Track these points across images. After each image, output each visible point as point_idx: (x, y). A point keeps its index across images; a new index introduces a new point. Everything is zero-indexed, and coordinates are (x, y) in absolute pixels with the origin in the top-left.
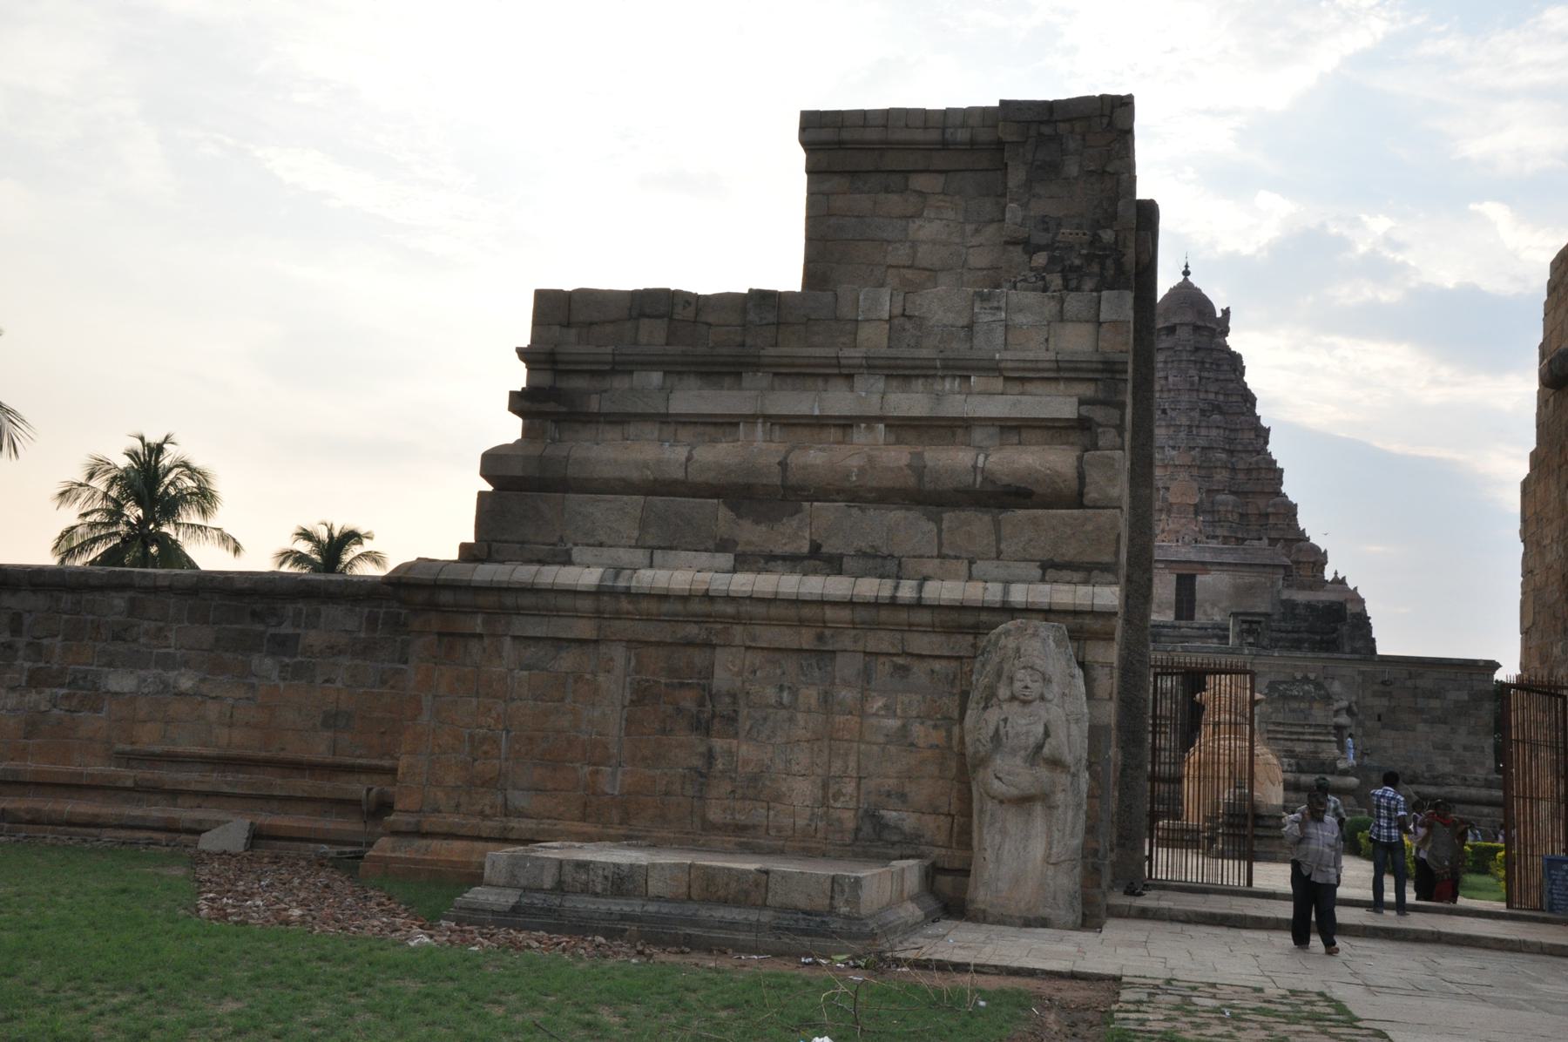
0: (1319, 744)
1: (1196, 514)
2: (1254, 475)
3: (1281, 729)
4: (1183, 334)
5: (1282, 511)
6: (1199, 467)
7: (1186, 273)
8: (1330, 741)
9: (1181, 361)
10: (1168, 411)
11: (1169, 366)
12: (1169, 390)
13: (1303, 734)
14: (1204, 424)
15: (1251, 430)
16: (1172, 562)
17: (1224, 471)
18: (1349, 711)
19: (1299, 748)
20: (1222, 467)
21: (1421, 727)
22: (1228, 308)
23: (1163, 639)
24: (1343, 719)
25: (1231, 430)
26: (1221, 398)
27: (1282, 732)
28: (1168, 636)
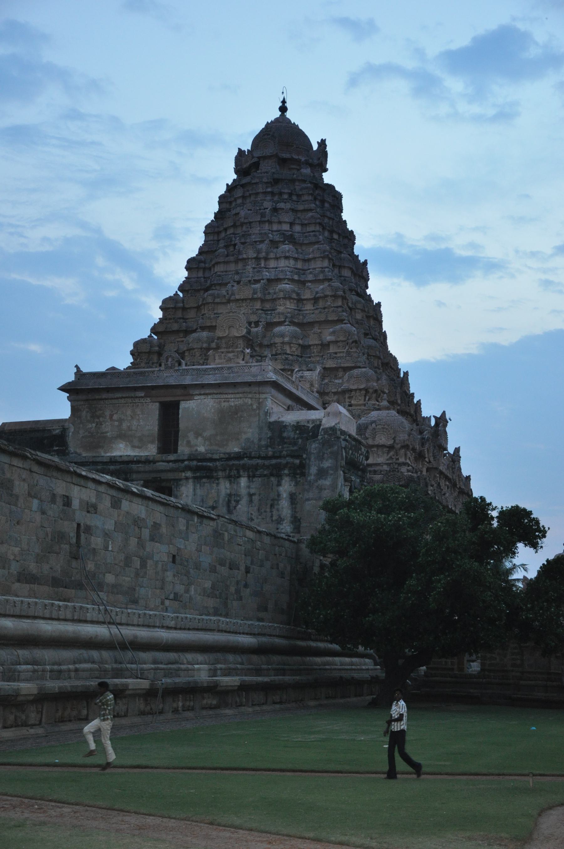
2: (321, 304)
5: (342, 338)
6: (263, 301)
7: (283, 109)
9: (257, 194)
12: (242, 224)
14: (272, 255)
15: (323, 258)
17: (288, 302)
20: (284, 298)
23: (134, 476)
25: (305, 261)
26: (297, 228)
28: (138, 472)
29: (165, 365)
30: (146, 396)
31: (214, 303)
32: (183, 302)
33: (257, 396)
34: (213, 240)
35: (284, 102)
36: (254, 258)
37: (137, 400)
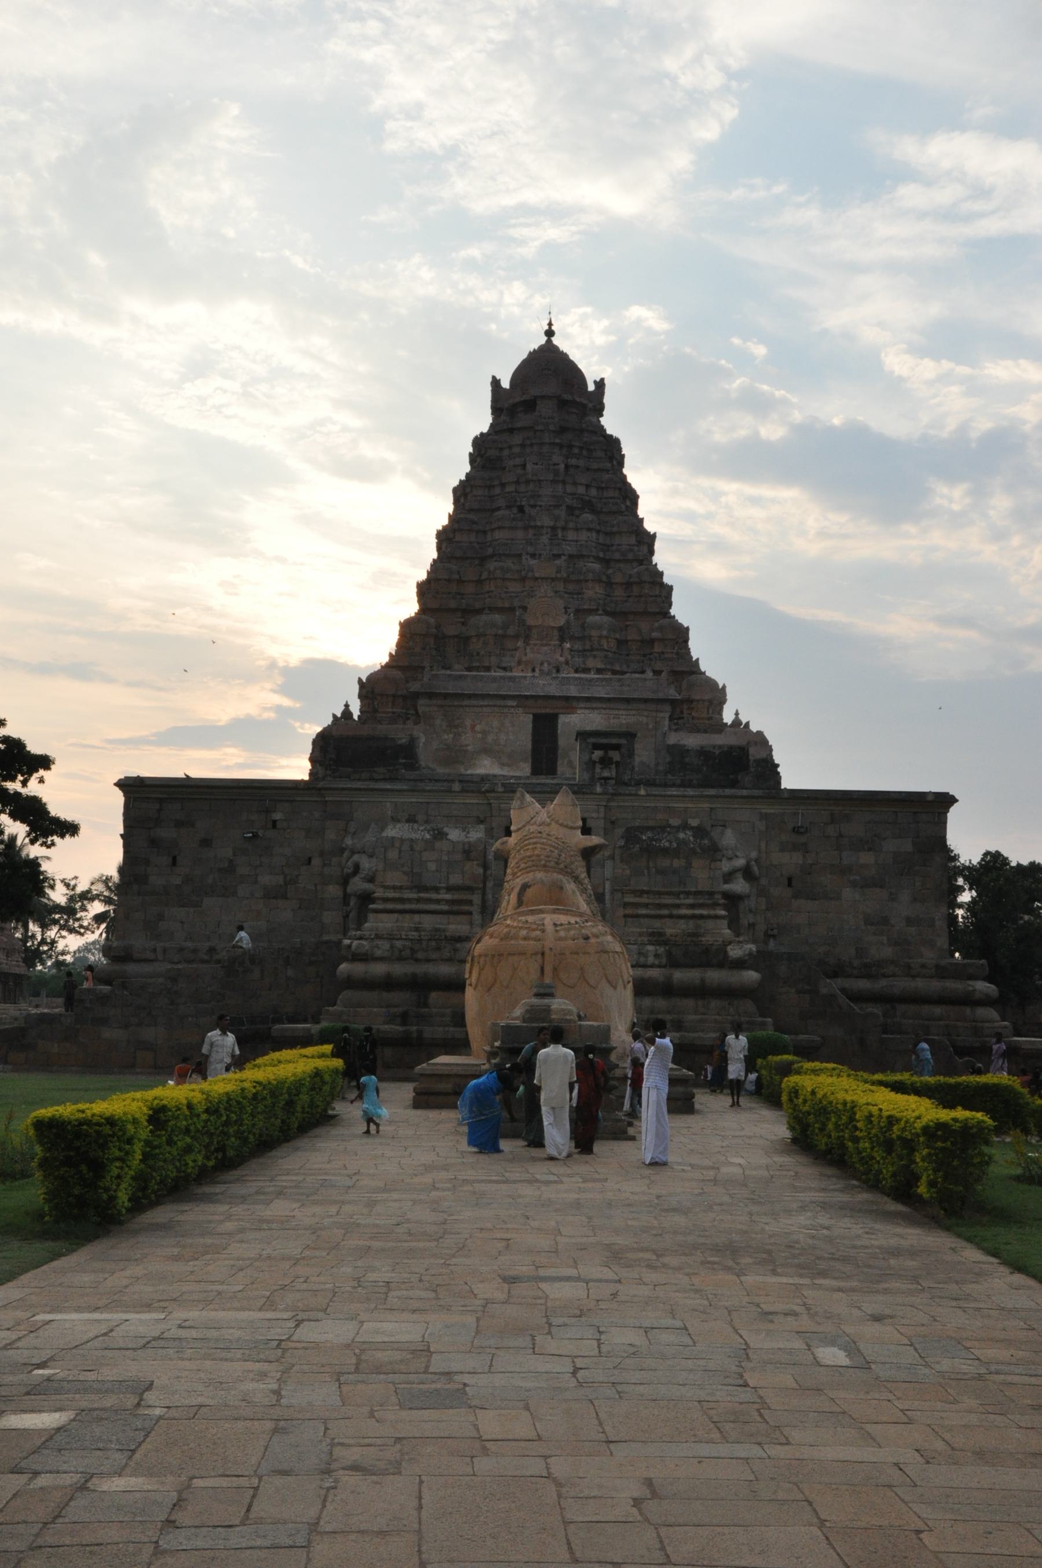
0: (700, 922)
1: (562, 640)
2: (636, 590)
3: (644, 900)
4: (545, 409)
6: (566, 581)
7: (550, 333)
8: (716, 917)
9: (542, 444)
10: (527, 509)
11: (528, 450)
12: (528, 482)
13: (678, 906)
14: (571, 525)
16: (526, 697)
18: (747, 873)
19: (672, 929)
21: (847, 893)
22: (602, 380)
24: (739, 886)
25: (606, 534)
26: (593, 492)
27: (646, 906)
29: (540, 670)
30: (518, 706)
31: (504, 579)
32: (459, 573)
33: (654, 714)
34: (485, 496)
35: (550, 324)
36: (550, 527)
37: (506, 710)
